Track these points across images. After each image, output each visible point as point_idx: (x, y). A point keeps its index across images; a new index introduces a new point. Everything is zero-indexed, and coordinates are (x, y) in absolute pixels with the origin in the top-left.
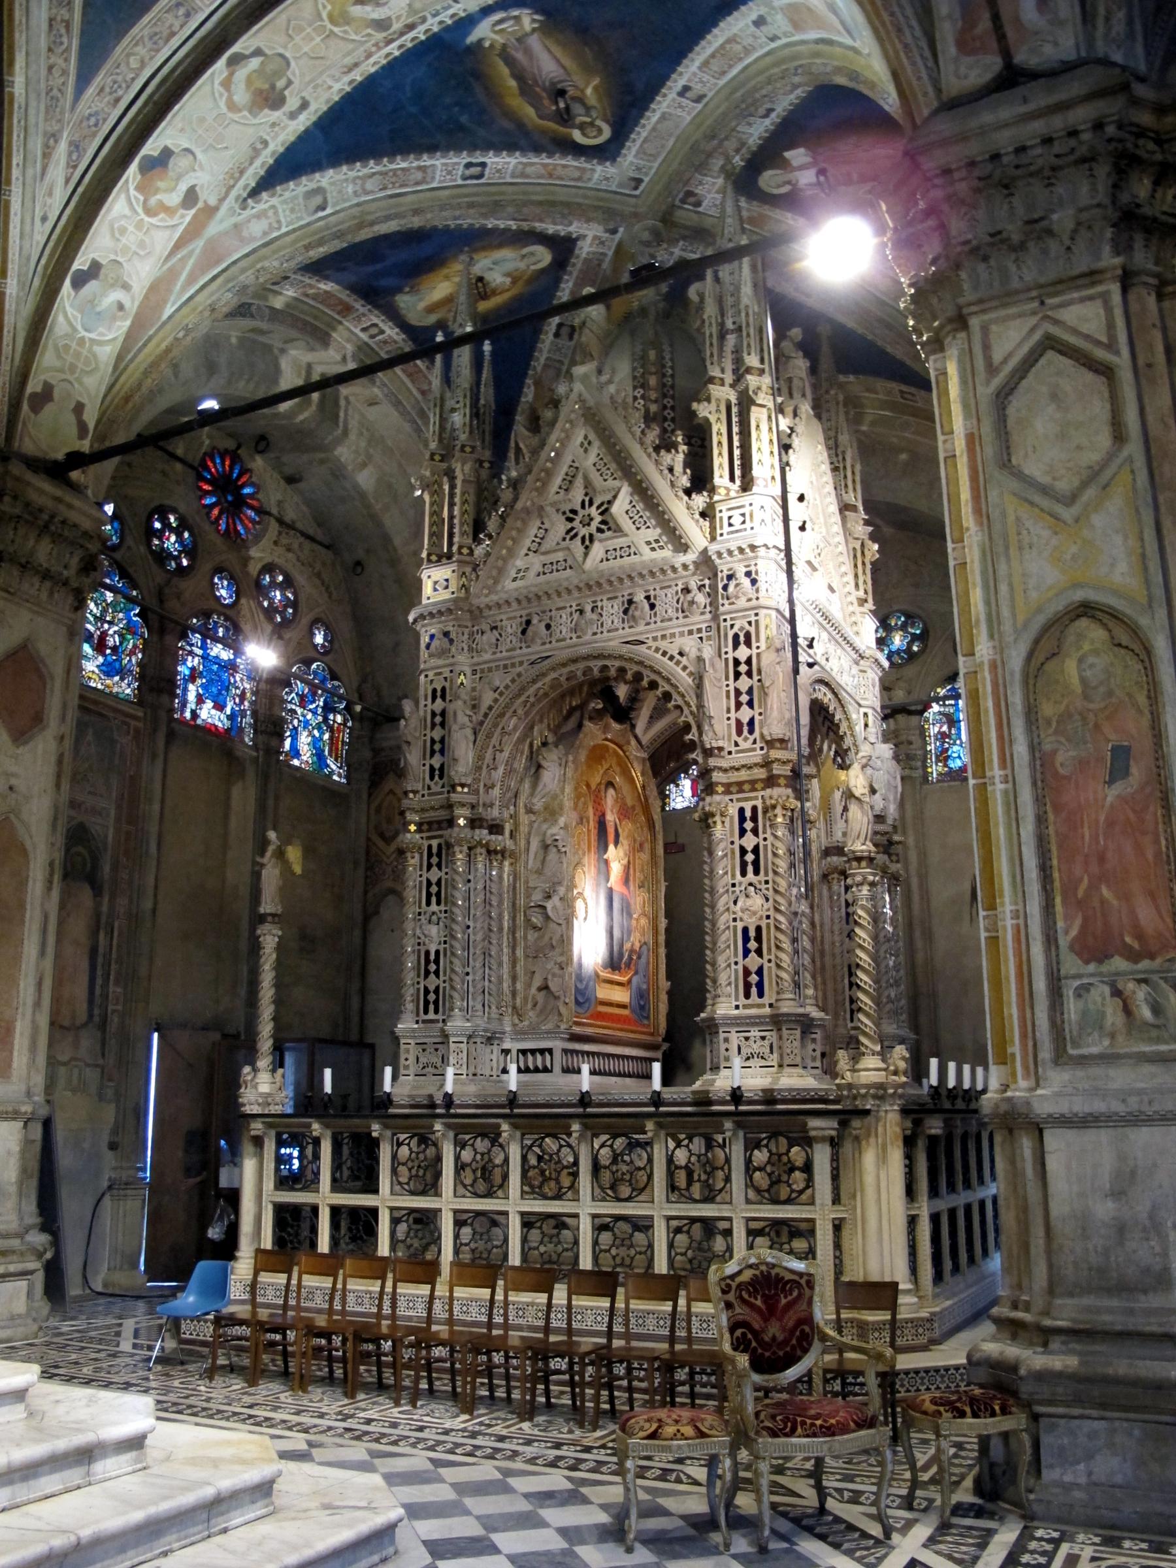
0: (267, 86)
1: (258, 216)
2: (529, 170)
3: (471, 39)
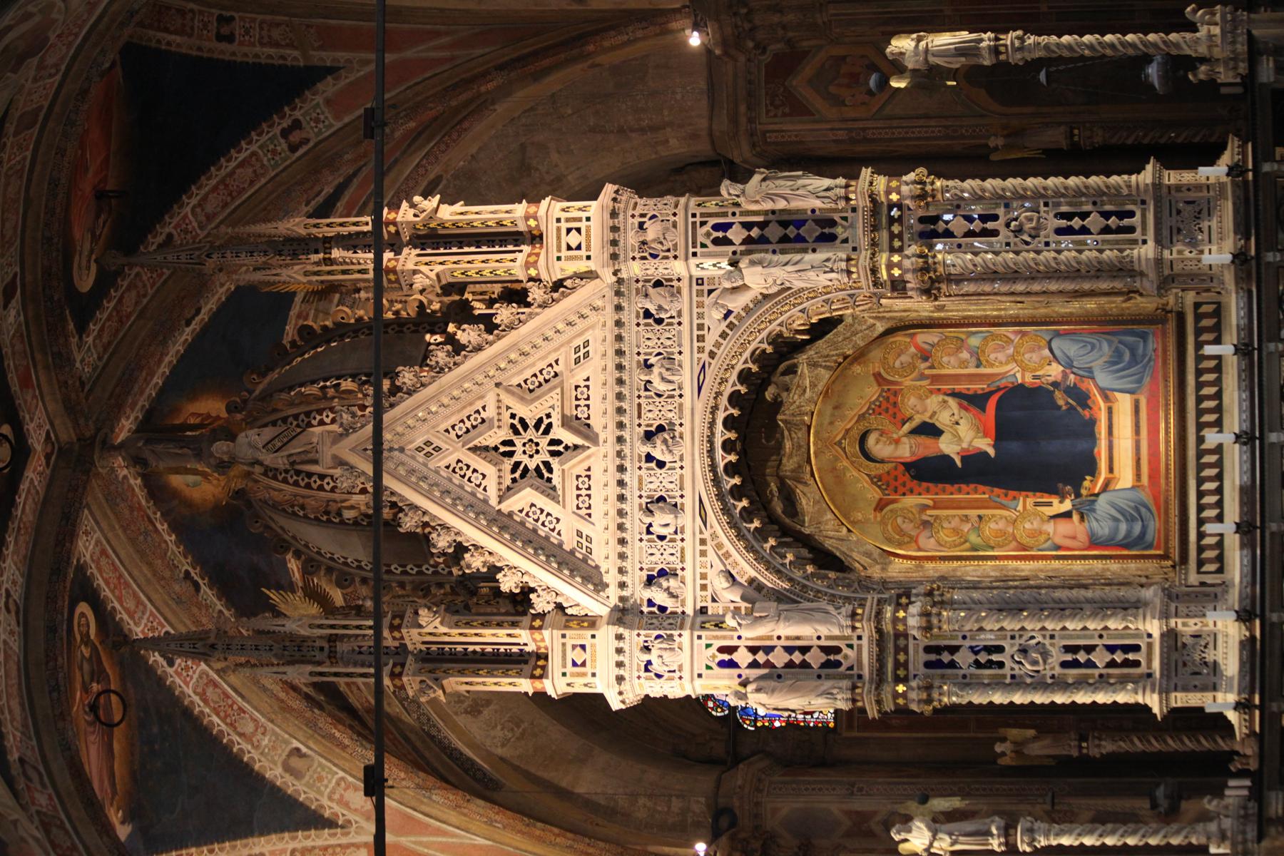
1: (346, 805)
2: (131, 604)
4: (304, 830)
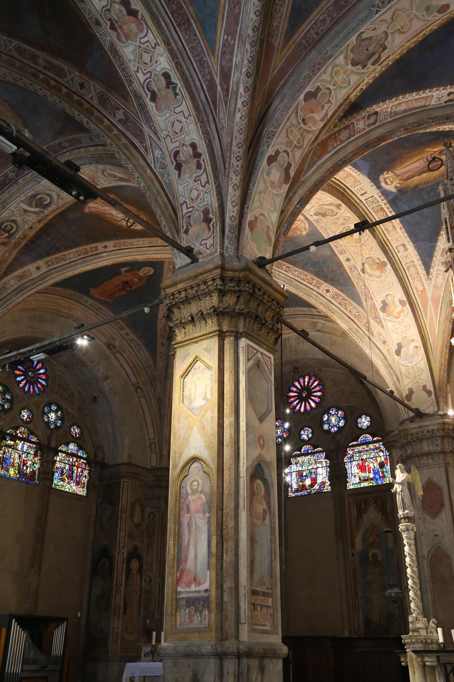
0: (377, 265)
1: (437, 277)
3: (394, 190)
4: (423, 263)
